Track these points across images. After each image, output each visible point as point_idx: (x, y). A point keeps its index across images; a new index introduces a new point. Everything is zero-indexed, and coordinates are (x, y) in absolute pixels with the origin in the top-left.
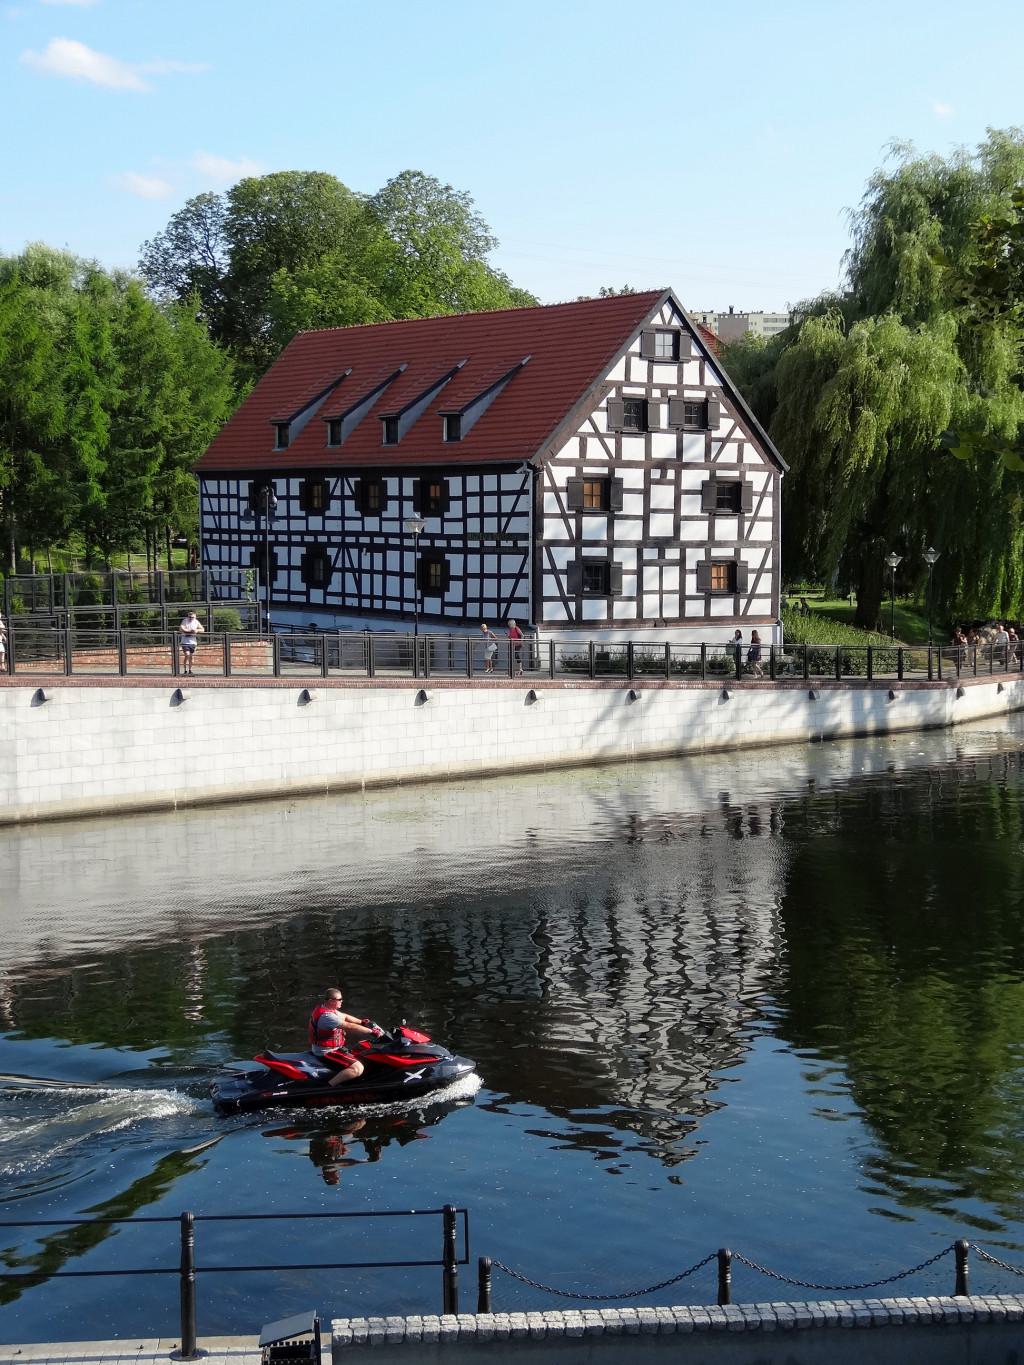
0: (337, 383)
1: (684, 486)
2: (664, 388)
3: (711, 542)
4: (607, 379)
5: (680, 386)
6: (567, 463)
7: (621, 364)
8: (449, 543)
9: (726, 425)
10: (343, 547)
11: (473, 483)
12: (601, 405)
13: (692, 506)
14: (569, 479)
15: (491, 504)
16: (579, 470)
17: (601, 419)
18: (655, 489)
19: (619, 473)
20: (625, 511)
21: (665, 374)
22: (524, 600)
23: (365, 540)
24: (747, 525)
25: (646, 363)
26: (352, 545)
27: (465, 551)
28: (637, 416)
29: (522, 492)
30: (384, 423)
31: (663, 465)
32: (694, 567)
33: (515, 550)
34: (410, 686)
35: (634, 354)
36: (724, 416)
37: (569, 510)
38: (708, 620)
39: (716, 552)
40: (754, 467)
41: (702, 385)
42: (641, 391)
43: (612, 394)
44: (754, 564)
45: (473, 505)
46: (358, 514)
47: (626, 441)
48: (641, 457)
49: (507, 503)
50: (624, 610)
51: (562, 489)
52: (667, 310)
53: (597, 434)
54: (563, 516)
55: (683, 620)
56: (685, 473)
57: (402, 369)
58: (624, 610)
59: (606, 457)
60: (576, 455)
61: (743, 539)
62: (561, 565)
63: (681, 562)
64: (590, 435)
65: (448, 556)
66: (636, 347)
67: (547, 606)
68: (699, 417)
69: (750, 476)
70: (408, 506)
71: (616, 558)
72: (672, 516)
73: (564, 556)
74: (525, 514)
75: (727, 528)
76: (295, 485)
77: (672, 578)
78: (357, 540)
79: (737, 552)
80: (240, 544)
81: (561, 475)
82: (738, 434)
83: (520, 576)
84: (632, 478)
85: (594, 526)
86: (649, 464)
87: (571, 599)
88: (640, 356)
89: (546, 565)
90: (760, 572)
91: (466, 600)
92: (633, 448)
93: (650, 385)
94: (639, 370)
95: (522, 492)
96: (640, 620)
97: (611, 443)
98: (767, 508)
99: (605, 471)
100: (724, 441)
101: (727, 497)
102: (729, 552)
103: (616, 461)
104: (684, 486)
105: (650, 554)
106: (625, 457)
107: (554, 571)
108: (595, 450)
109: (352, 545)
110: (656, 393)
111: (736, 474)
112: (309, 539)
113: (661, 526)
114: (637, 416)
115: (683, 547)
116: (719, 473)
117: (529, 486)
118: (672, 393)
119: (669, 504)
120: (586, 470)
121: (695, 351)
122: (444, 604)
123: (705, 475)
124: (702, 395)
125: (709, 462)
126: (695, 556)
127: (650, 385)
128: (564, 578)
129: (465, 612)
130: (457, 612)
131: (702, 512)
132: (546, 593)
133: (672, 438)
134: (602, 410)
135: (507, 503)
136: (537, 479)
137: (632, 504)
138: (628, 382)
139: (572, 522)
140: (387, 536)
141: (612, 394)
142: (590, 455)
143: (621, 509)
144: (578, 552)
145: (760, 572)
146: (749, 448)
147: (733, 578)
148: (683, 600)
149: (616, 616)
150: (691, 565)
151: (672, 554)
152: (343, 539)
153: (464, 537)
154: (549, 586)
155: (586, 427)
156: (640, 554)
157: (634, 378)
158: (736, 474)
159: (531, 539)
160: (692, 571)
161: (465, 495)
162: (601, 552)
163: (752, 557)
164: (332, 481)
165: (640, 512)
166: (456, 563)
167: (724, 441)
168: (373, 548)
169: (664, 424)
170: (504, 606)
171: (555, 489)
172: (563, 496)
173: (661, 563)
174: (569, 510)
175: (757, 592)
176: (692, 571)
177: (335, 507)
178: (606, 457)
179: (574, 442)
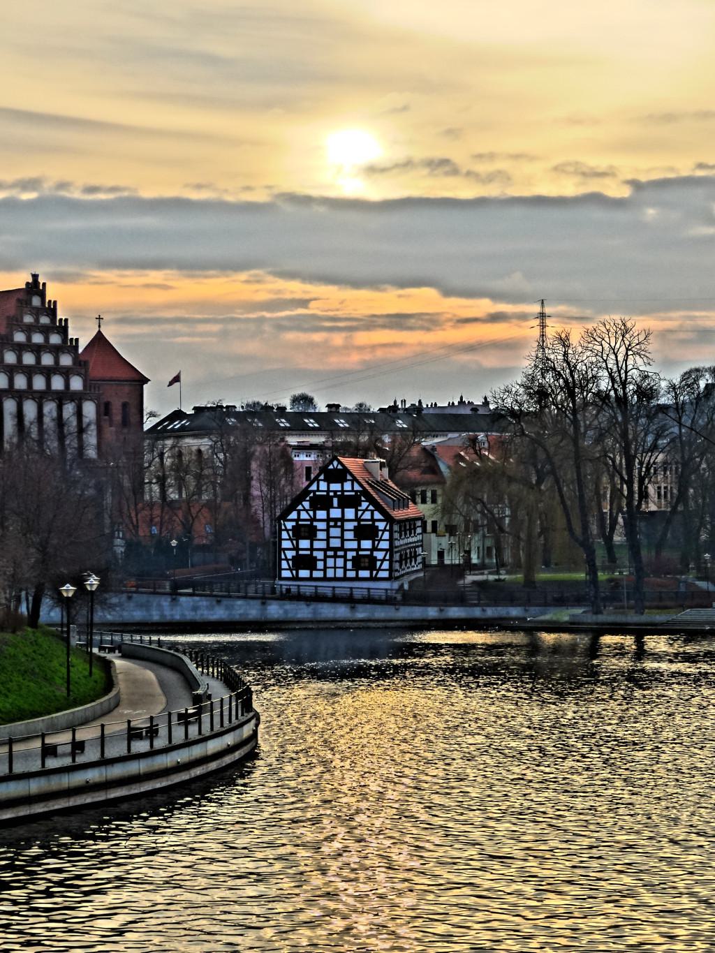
1: (345, 528)
2: (335, 492)
3: (359, 549)
4: (311, 489)
5: (343, 491)
7: (315, 484)
9: (365, 505)
16: (297, 523)
17: (306, 504)
18: (331, 529)
19: (315, 524)
21: (335, 487)
24: (376, 543)
25: (326, 483)
28: (322, 502)
31: (336, 520)
32: (351, 558)
35: (322, 480)
36: (364, 501)
38: (357, 579)
39: (361, 553)
41: (353, 490)
42: (325, 493)
47: (317, 512)
48: (325, 517)
50: (317, 574)
51: (290, 530)
52: (335, 463)
53: (305, 510)
54: (290, 539)
55: (345, 579)
56: (345, 523)
58: (317, 574)
60: (296, 518)
61: (375, 549)
63: (345, 557)
64: (302, 510)
66: (322, 477)
67: (283, 572)
69: (377, 524)
72: (339, 540)
73: (290, 554)
75: (367, 544)
77: (340, 562)
79: (372, 553)
81: (289, 525)
82: (371, 508)
85: (304, 544)
86: (328, 520)
88: (324, 480)
89: (283, 557)
90: (383, 560)
92: (321, 514)
94: (323, 486)
96: (325, 579)
97: (311, 513)
98: (386, 536)
99: (309, 523)
100: (364, 511)
102: (368, 553)
103: (314, 519)
104: (345, 528)
106: (318, 517)
107: (286, 559)
108: (304, 515)
113: (335, 543)
114: (322, 502)
115: (346, 551)
116: (362, 523)
119: (339, 534)
120: (300, 523)
121: (349, 477)
123: (356, 524)
124: (353, 493)
125: (357, 519)
126: (350, 555)
127: (328, 491)
131: (355, 537)
132: (283, 567)
133: (340, 510)
134: (307, 501)
137: (321, 535)
138: (318, 490)
139: (294, 542)
141: (312, 495)
142: (302, 517)
143: (316, 536)
144: (297, 553)
145: (383, 560)
147: (371, 563)
148: (345, 568)
149: (314, 576)
154: (284, 564)
155: (300, 507)
156: (325, 554)
157: (320, 489)
158: (370, 523)
160: (349, 560)
162: (308, 552)
163: (379, 555)
165: (325, 538)
167: (364, 511)
171: (287, 530)
172: (291, 533)
173: (335, 556)
175: (382, 568)
176: (349, 560)
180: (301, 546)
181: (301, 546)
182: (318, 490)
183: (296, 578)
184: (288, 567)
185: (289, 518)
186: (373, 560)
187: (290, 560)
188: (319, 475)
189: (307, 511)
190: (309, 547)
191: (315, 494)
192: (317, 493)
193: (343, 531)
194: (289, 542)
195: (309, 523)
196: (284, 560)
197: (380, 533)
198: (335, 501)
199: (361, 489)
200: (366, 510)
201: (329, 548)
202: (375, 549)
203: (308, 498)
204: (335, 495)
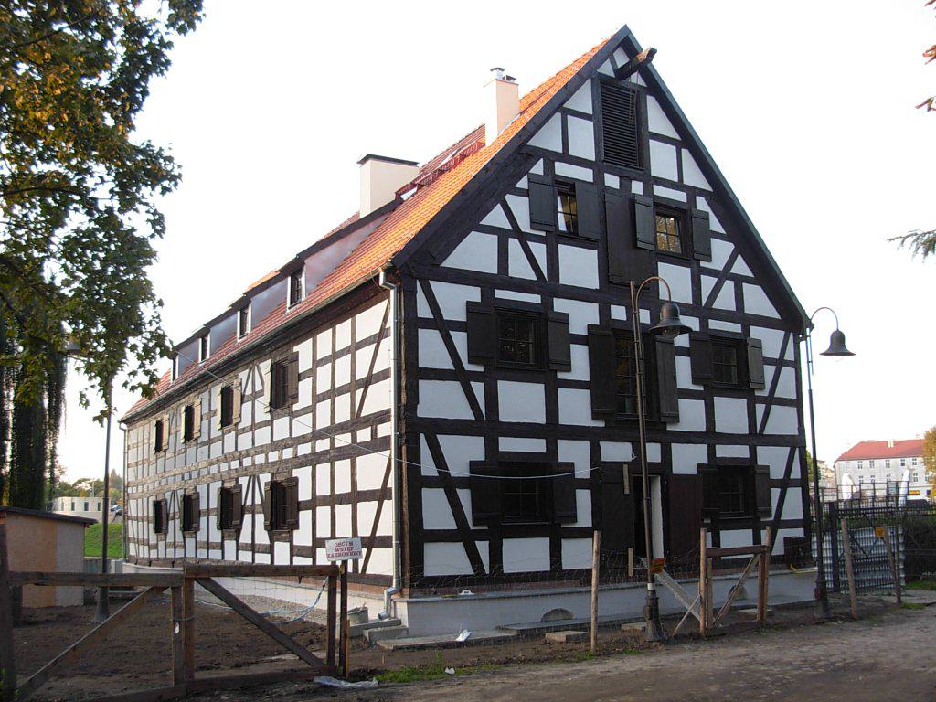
4: (533, 142)
12: (519, 185)
14: (470, 306)
19: (560, 305)
22: (384, 542)
27: (313, 460)
29: (383, 334)
33: (377, 445)
37: (470, 362)
51: (458, 326)
53: (517, 232)
54: (458, 374)
59: (532, 276)
62: (458, 469)
65: (296, 473)
71: (561, 459)
73: (463, 453)
74: (384, 375)
81: (454, 300)
87: (481, 536)
91: (318, 543)
99: (536, 299)
106: (566, 278)
107: (446, 482)
120: (499, 294)
122: (294, 551)
129: (314, 561)
130: (308, 561)
132: (429, 524)
139: (478, 388)
141: (538, 168)
143: (567, 367)
144: (491, 446)
149: (567, 565)
154: (436, 511)
155: (496, 217)
159: (393, 418)
162: (537, 446)
171: (443, 326)
172: (460, 339)
174: (470, 362)
178: (532, 276)
180: (506, 415)
181: (506, 415)
182: (566, 157)
183: (489, 579)
184: (452, 526)
185: (452, 261)
187: (462, 482)
188: (570, 89)
189: (524, 239)
190: (541, 419)
191: (549, 168)
194: (455, 387)
195: (536, 299)
196: (431, 482)
197: (769, 371)
203: (523, 183)
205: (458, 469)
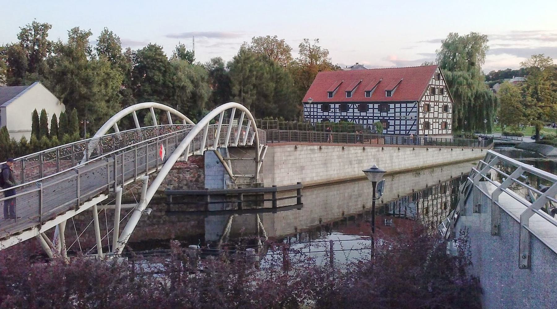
0: (341, 84)
5: (439, 85)
6: (423, 101)
8: (389, 118)
10: (353, 119)
11: (398, 105)
13: (440, 110)
15: (404, 110)
17: (428, 92)
20: (431, 112)
21: (437, 83)
23: (362, 117)
26: (356, 119)
27: (395, 120)
28: (433, 92)
29: (414, 107)
30: (366, 93)
31: (437, 102)
34: (425, 147)
38: (442, 134)
40: (449, 102)
42: (434, 86)
43: (430, 87)
44: (449, 123)
45: (398, 110)
46: (359, 112)
49: (409, 110)
53: (428, 95)
57: (362, 80)
61: (447, 118)
62: (422, 123)
65: (388, 121)
66: (433, 77)
68: (442, 92)
70: (376, 111)
72: (437, 113)
73: (422, 121)
75: (445, 114)
76: (337, 106)
78: (358, 117)
80: (317, 118)
82: (447, 96)
83: (414, 125)
84: (432, 104)
86: (435, 101)
90: (450, 124)
92: (432, 97)
93: (435, 85)
95: (414, 107)
96: (433, 134)
97: (429, 97)
98: (451, 111)
101: (445, 109)
102: (445, 120)
103: (430, 101)
105: (434, 120)
107: (421, 124)
108: (427, 99)
109: (356, 119)
110: (436, 87)
111: (447, 104)
112: (340, 117)
113: (436, 116)
117: (417, 106)
118: (438, 87)
121: (442, 78)
124: (442, 87)
125: (443, 102)
126: (441, 121)
128: (422, 125)
132: (420, 129)
135: (409, 110)
136: (419, 105)
140: (368, 117)
141: (430, 87)
144: (424, 120)
145: (450, 124)
146: (448, 98)
150: (440, 123)
151: (437, 121)
152: (353, 117)
153: (395, 117)
154: (420, 128)
155: (426, 94)
158: (447, 104)
161: (395, 108)
164: (350, 105)
166: (392, 123)
167: (445, 97)
168: (363, 119)
169: (437, 94)
170: (407, 132)
173: (436, 122)
177: (351, 110)
179: (424, 96)
186: (446, 123)
192: (432, 86)
193: (439, 107)
198: (437, 90)
199: (445, 85)
200: (445, 97)
201: (434, 118)
202: (447, 118)
204: (438, 88)
205: (422, 123)
